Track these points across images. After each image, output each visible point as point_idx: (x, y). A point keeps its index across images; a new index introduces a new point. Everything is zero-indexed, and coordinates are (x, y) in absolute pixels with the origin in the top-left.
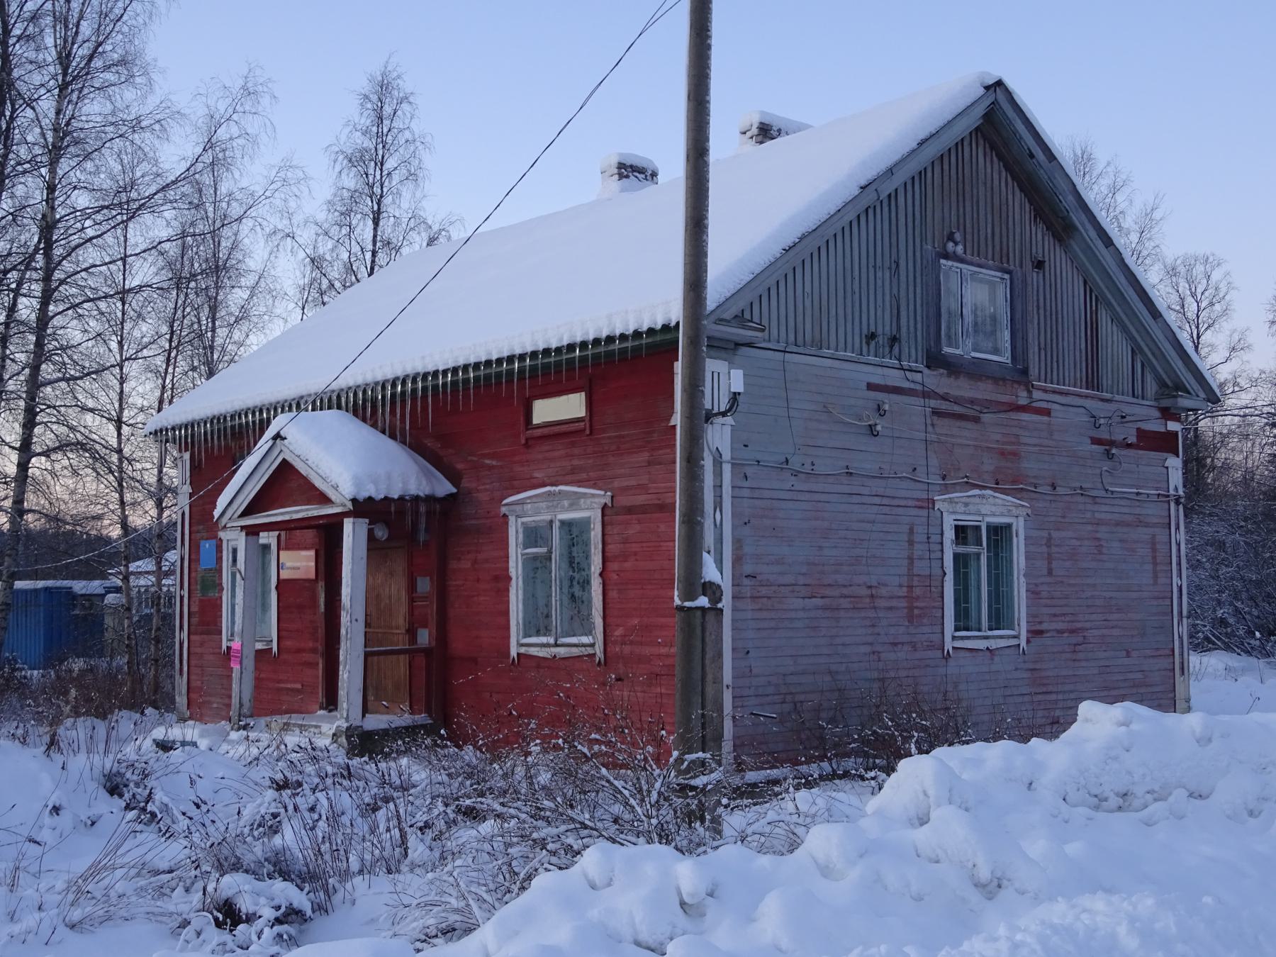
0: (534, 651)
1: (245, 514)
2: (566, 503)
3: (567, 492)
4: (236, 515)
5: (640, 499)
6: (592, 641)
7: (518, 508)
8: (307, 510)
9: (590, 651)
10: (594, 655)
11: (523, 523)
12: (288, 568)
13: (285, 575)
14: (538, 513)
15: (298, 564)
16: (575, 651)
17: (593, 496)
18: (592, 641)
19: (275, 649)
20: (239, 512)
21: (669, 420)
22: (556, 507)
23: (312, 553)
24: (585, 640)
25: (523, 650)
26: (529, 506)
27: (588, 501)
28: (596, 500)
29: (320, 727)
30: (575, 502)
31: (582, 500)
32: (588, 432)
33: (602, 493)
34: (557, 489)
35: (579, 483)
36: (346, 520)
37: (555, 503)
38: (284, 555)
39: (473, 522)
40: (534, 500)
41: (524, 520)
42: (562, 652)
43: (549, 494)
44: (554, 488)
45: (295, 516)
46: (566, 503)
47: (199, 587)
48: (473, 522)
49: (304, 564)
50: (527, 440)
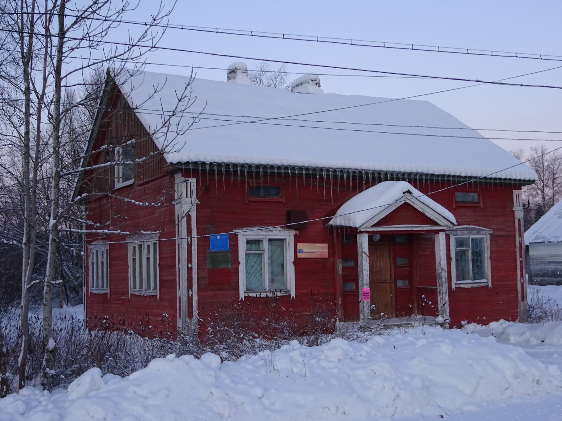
0: (462, 286)
1: (374, 226)
2: (475, 232)
3: (475, 228)
4: (370, 226)
5: (502, 233)
6: (487, 280)
7: (454, 232)
8: (422, 227)
9: (486, 284)
10: (488, 286)
11: (455, 238)
12: (305, 252)
13: (300, 255)
14: (463, 234)
15: (314, 250)
16: (482, 285)
17: (486, 230)
18: (487, 280)
19: (293, 294)
20: (373, 224)
21: (512, 208)
22: (471, 233)
23: (326, 245)
24: (485, 281)
25: (458, 286)
26: (459, 232)
27: (484, 232)
28: (488, 232)
29: (412, 324)
30: (479, 232)
31: (482, 231)
32: (482, 207)
33: (489, 229)
34: (471, 226)
35: (478, 225)
36: (440, 233)
37: (470, 232)
38: (300, 246)
39: (427, 236)
40: (461, 230)
41: (456, 237)
42: (475, 285)
43: (467, 228)
44: (468, 226)
45: (414, 229)
46: (475, 232)
47: (208, 262)
48: (427, 236)
49: (319, 250)
50: (456, 206)
